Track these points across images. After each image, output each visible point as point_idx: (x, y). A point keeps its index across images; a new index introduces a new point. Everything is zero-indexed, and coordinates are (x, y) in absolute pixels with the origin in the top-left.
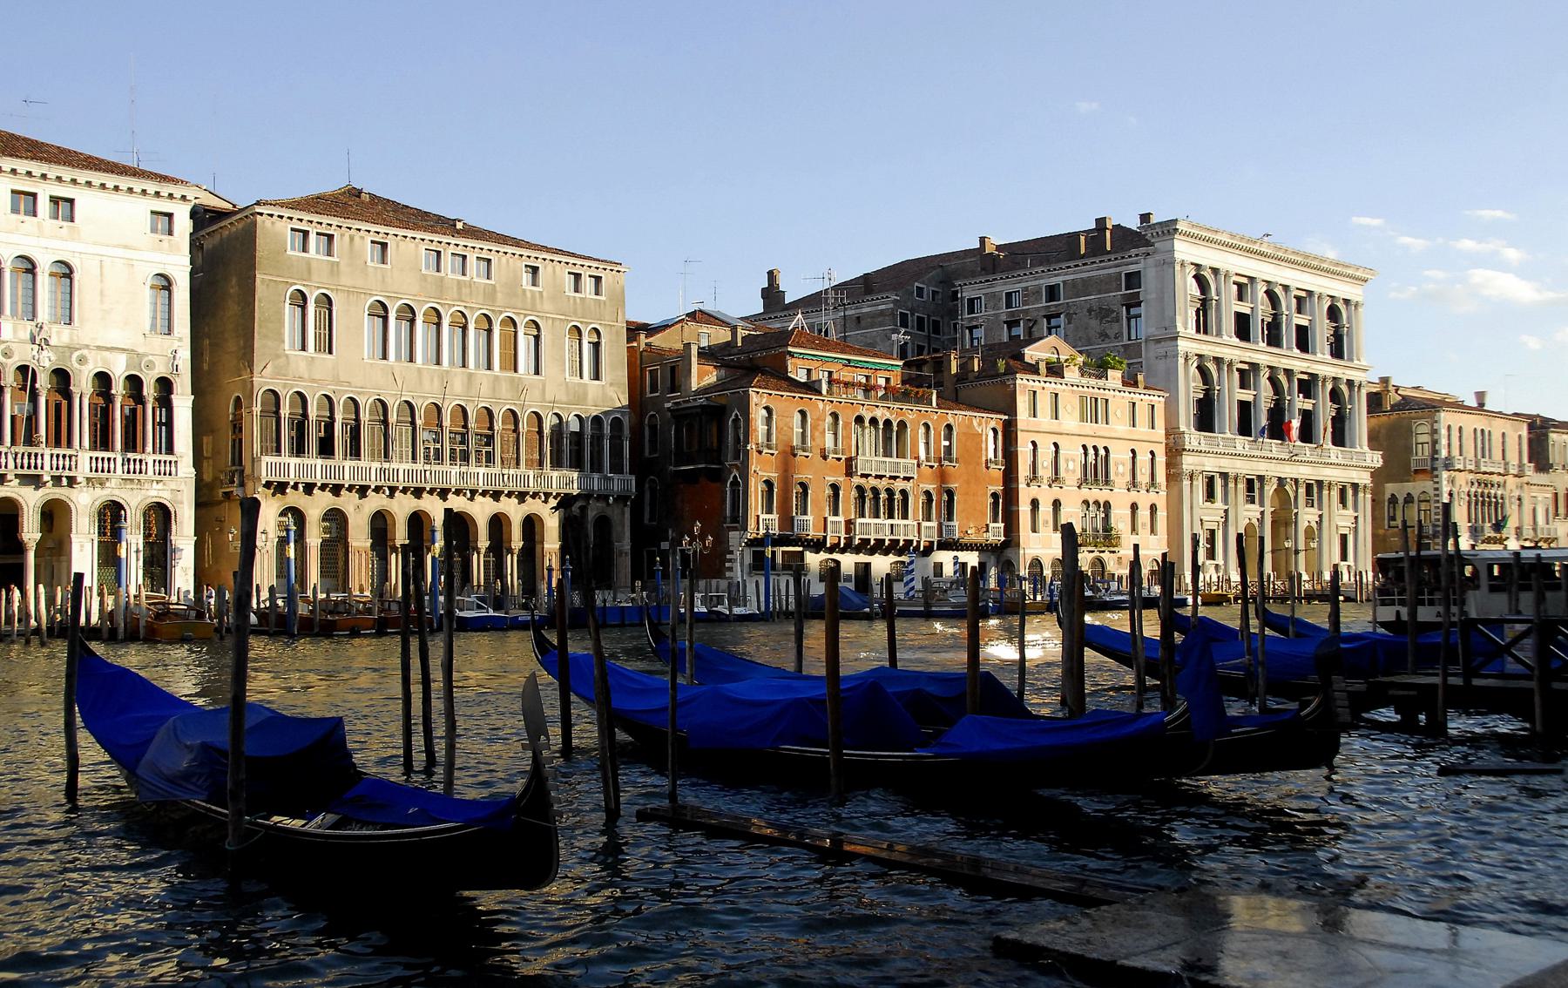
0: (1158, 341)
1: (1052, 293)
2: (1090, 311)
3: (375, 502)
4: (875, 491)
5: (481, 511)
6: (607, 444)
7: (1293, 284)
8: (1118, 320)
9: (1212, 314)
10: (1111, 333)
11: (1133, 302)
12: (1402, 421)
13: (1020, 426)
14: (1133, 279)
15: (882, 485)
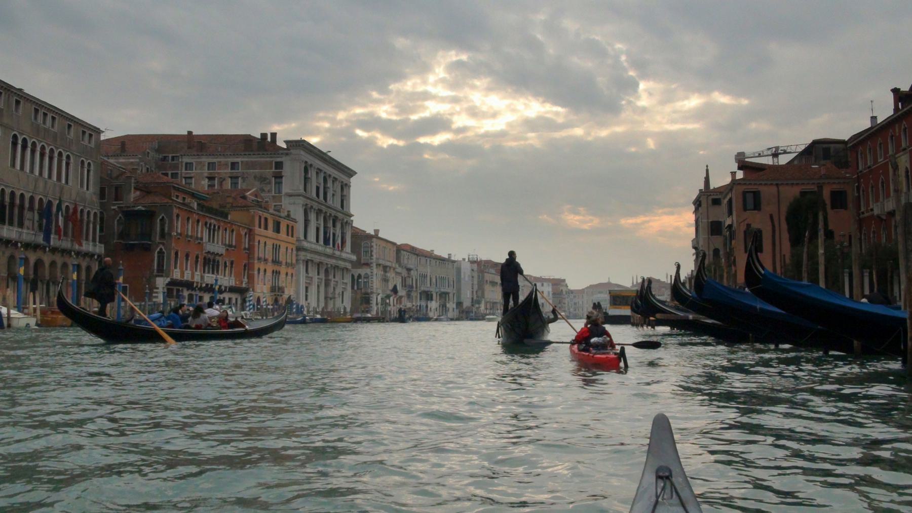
0: (291, 196)
1: (234, 165)
2: (255, 177)
3: (39, 254)
4: (209, 259)
5: (47, 259)
6: (91, 226)
7: (333, 175)
8: (270, 183)
9: (308, 186)
10: (266, 189)
11: (279, 177)
12: (362, 240)
13: (256, 232)
14: (279, 165)
15: (212, 257)
